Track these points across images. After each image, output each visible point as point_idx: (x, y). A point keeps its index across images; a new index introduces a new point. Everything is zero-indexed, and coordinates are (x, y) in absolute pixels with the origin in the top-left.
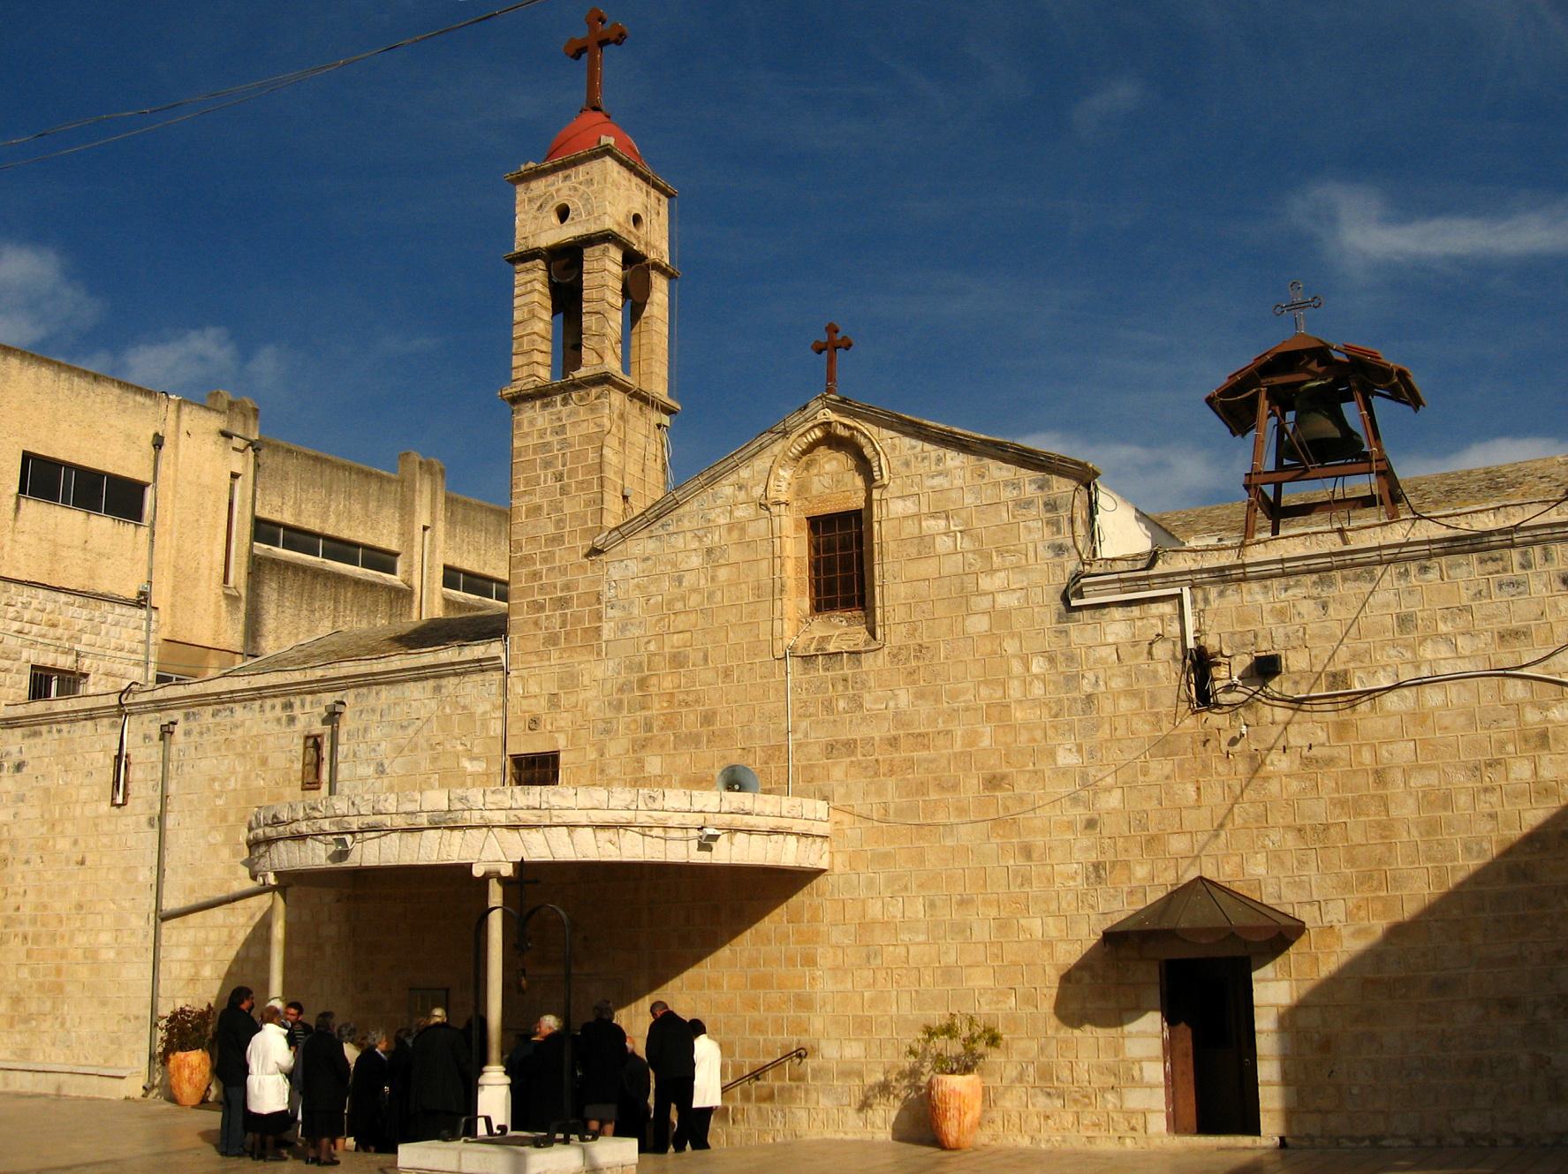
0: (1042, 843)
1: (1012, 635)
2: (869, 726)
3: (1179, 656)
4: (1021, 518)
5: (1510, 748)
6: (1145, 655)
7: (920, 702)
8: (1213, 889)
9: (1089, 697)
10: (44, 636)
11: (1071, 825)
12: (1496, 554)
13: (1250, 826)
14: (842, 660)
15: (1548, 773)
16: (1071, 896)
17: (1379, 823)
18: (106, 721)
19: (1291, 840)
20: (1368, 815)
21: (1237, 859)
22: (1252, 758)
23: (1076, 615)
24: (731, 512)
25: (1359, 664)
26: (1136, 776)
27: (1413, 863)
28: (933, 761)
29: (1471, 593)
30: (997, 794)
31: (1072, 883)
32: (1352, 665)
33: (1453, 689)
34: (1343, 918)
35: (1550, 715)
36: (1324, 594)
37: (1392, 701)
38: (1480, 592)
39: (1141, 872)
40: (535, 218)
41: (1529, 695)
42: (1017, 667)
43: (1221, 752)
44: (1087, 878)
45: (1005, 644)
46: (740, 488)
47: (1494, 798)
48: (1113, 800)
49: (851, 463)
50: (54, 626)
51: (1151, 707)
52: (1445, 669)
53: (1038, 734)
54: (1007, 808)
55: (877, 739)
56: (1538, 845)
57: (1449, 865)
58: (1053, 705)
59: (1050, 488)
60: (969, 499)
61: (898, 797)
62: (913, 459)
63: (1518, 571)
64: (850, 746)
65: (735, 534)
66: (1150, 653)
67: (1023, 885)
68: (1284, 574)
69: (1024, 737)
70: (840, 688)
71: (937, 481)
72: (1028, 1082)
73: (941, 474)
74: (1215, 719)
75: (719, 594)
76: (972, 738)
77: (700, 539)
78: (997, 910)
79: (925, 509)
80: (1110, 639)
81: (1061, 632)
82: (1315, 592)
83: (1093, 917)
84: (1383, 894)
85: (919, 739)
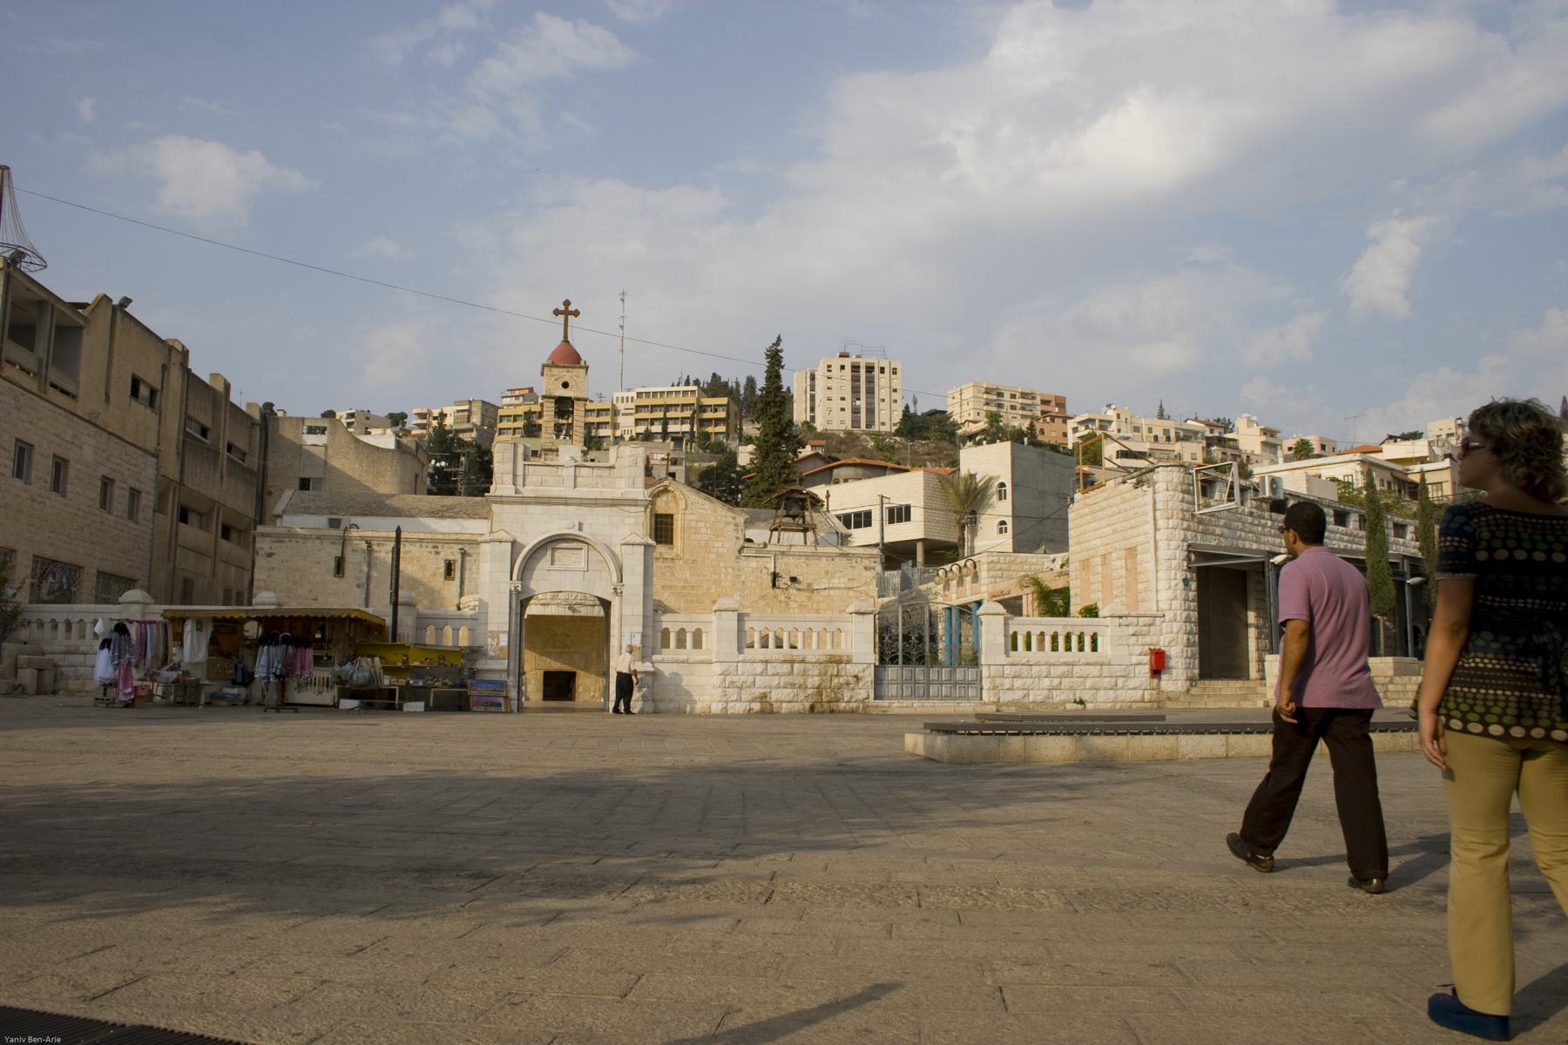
64: (670, 587)
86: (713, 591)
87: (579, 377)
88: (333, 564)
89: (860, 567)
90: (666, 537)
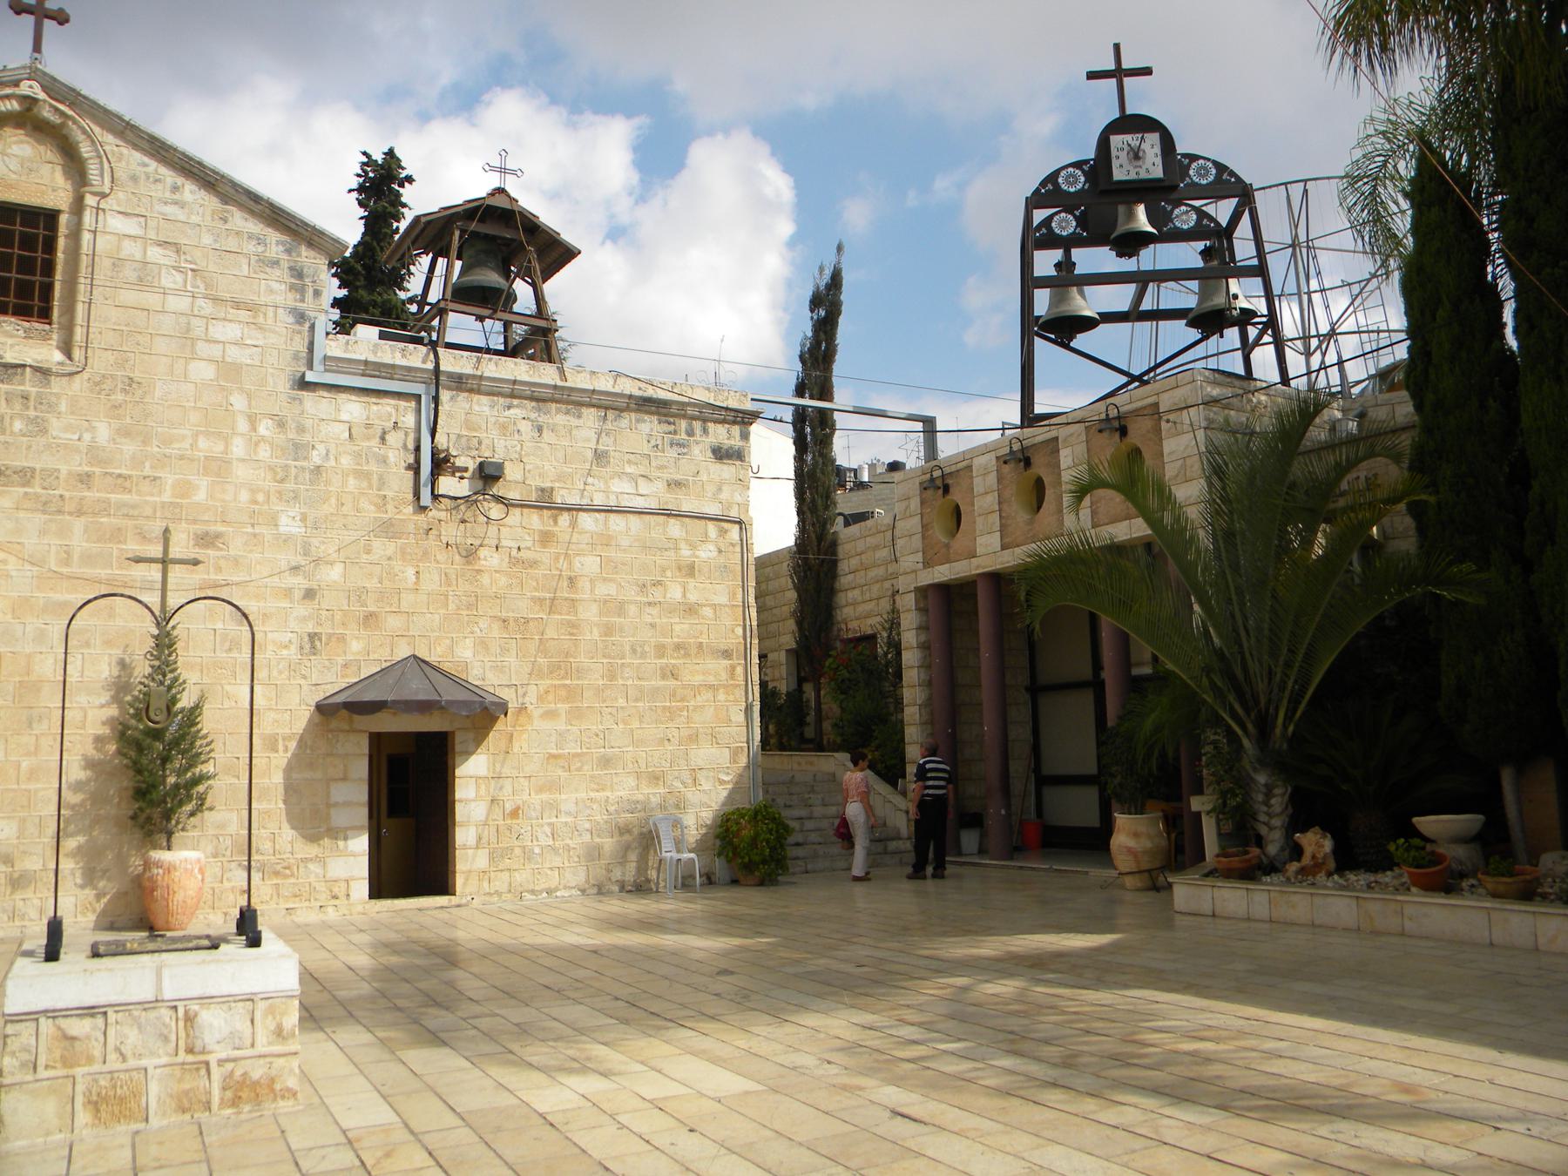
0: (256, 608)
1: (241, 390)
2: (54, 455)
4: (263, 276)
5: (669, 574)
6: (378, 439)
7: (123, 440)
8: (422, 665)
9: (318, 469)
11: (288, 593)
13: (462, 612)
14: (22, 374)
15: (693, 597)
16: (283, 664)
17: (569, 622)
19: (496, 631)
20: (561, 614)
21: (448, 642)
25: (562, 485)
26: (359, 553)
27: (593, 658)
28: (134, 507)
29: (650, 445)
30: (209, 552)
31: (285, 652)
32: (557, 485)
34: (534, 701)
35: (697, 553)
36: (540, 419)
37: (586, 520)
38: (657, 446)
39: (355, 646)
41: (684, 534)
42: (242, 425)
43: (441, 541)
44: (301, 648)
45: (232, 399)
47: (654, 611)
48: (334, 573)
51: (379, 490)
52: (626, 502)
53: (260, 497)
55: (65, 472)
56: (682, 652)
57: (620, 662)
58: (279, 470)
59: (299, 255)
60: (207, 240)
61: (87, 541)
62: (143, 177)
63: (684, 436)
66: (383, 439)
67: (230, 650)
68: (512, 396)
69: (244, 496)
70: (18, 407)
71: (170, 210)
72: (224, 855)
73: (176, 203)
76: (185, 489)
78: (199, 674)
79: (152, 235)
80: (344, 417)
81: (294, 399)
82: (533, 415)
83: (305, 688)
84: (568, 682)
85: (120, 481)
86: (201, 496)
89: (699, 453)
90: (24, 290)
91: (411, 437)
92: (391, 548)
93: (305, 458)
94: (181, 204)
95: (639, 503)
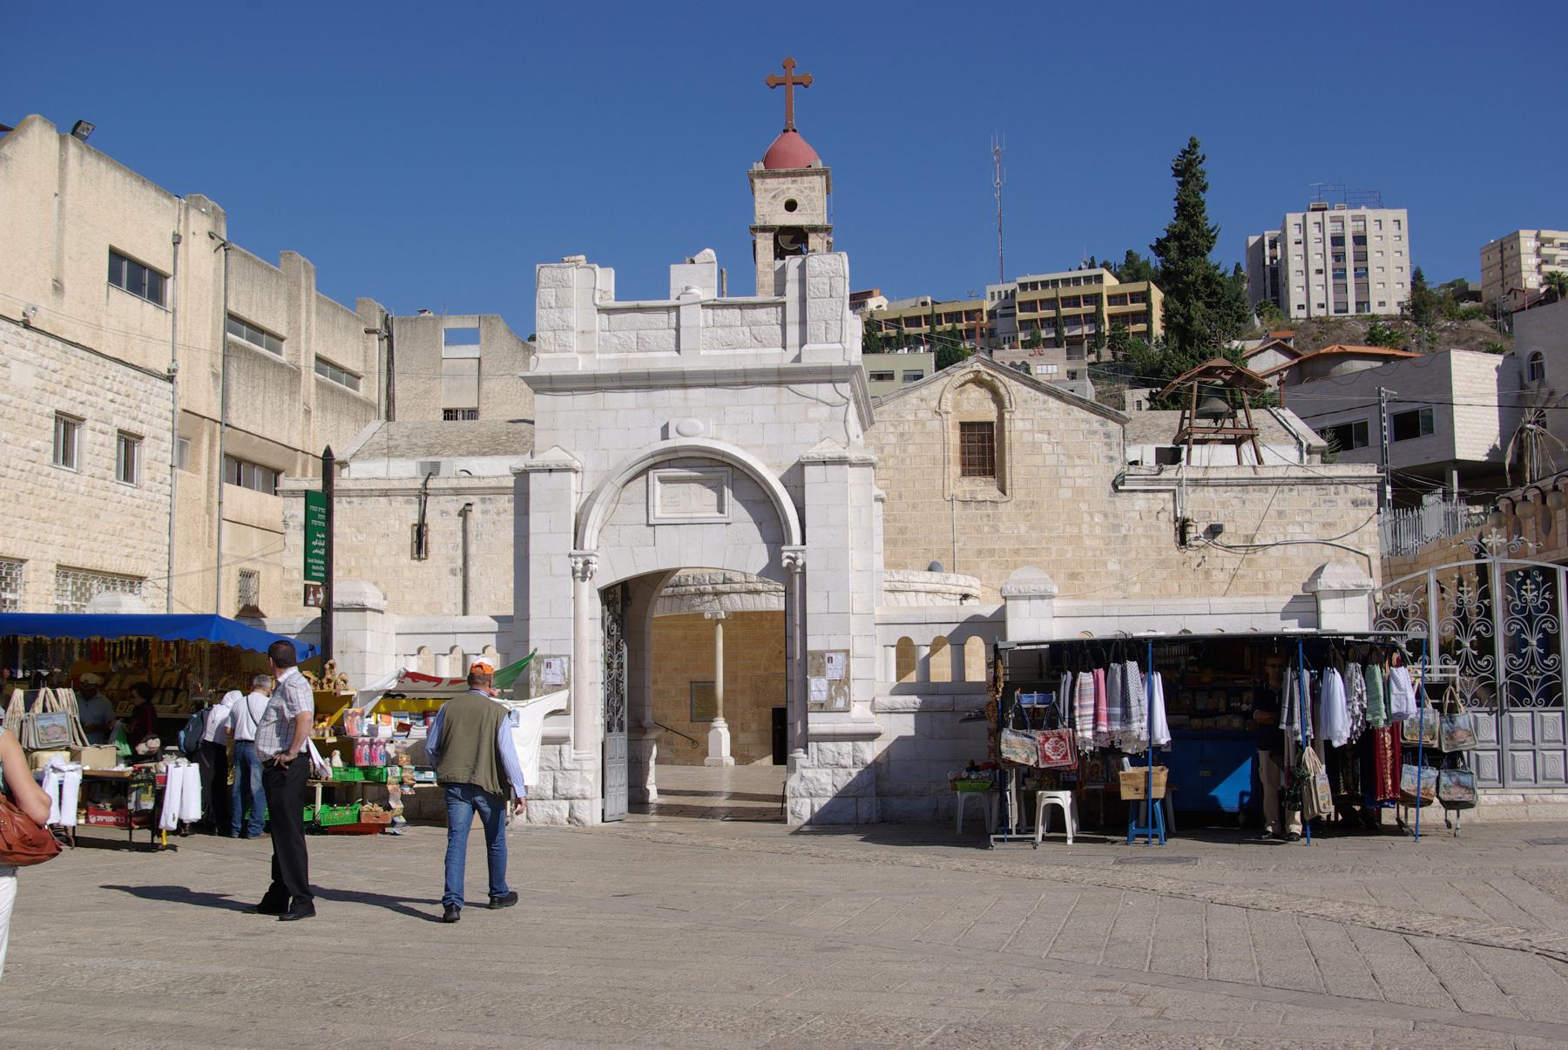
1: (1085, 501)
3: (1172, 520)
9: (1125, 536)
10: (123, 405)
12: (1324, 487)
18: (400, 498)
22: (1206, 572)
23: (1120, 494)
24: (916, 414)
33: (1301, 547)
37: (1272, 550)
40: (770, 203)
42: (1087, 518)
46: (922, 400)
49: (989, 395)
50: (128, 396)
52: (1298, 538)
53: (1098, 553)
54: (1080, 590)
59: (1107, 426)
60: (1062, 426)
64: (991, 552)
65: (919, 426)
66: (1157, 517)
68: (1227, 485)
69: (1090, 554)
71: (1043, 413)
74: (1189, 553)
75: (908, 459)
77: (895, 427)
79: (1036, 428)
80: (1137, 508)
82: (1240, 495)
86: (1069, 555)
87: (813, 189)
88: (408, 537)
91: (1172, 515)
92: (1165, 573)
93: (1119, 531)
94: (1048, 410)
95: (1307, 538)
